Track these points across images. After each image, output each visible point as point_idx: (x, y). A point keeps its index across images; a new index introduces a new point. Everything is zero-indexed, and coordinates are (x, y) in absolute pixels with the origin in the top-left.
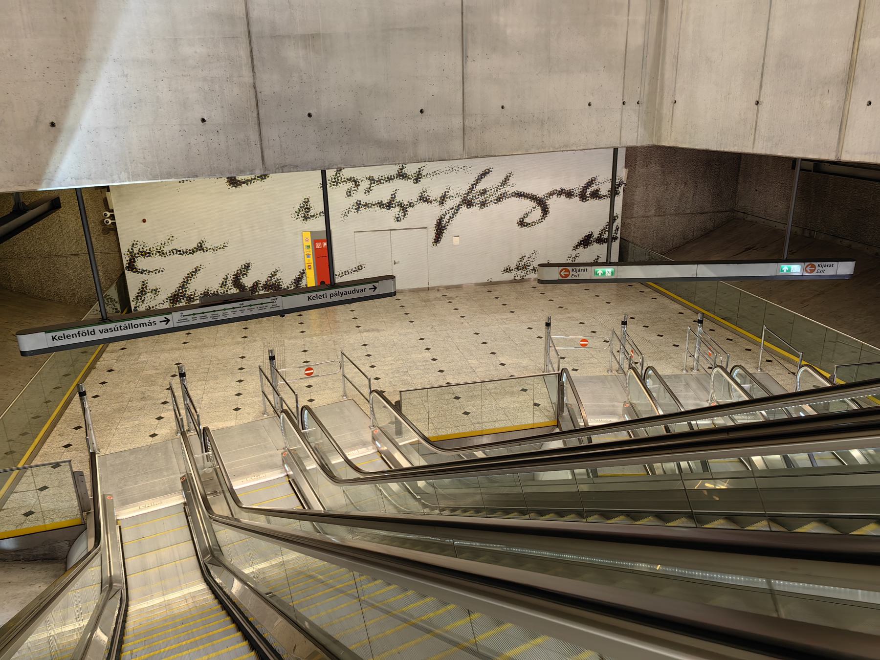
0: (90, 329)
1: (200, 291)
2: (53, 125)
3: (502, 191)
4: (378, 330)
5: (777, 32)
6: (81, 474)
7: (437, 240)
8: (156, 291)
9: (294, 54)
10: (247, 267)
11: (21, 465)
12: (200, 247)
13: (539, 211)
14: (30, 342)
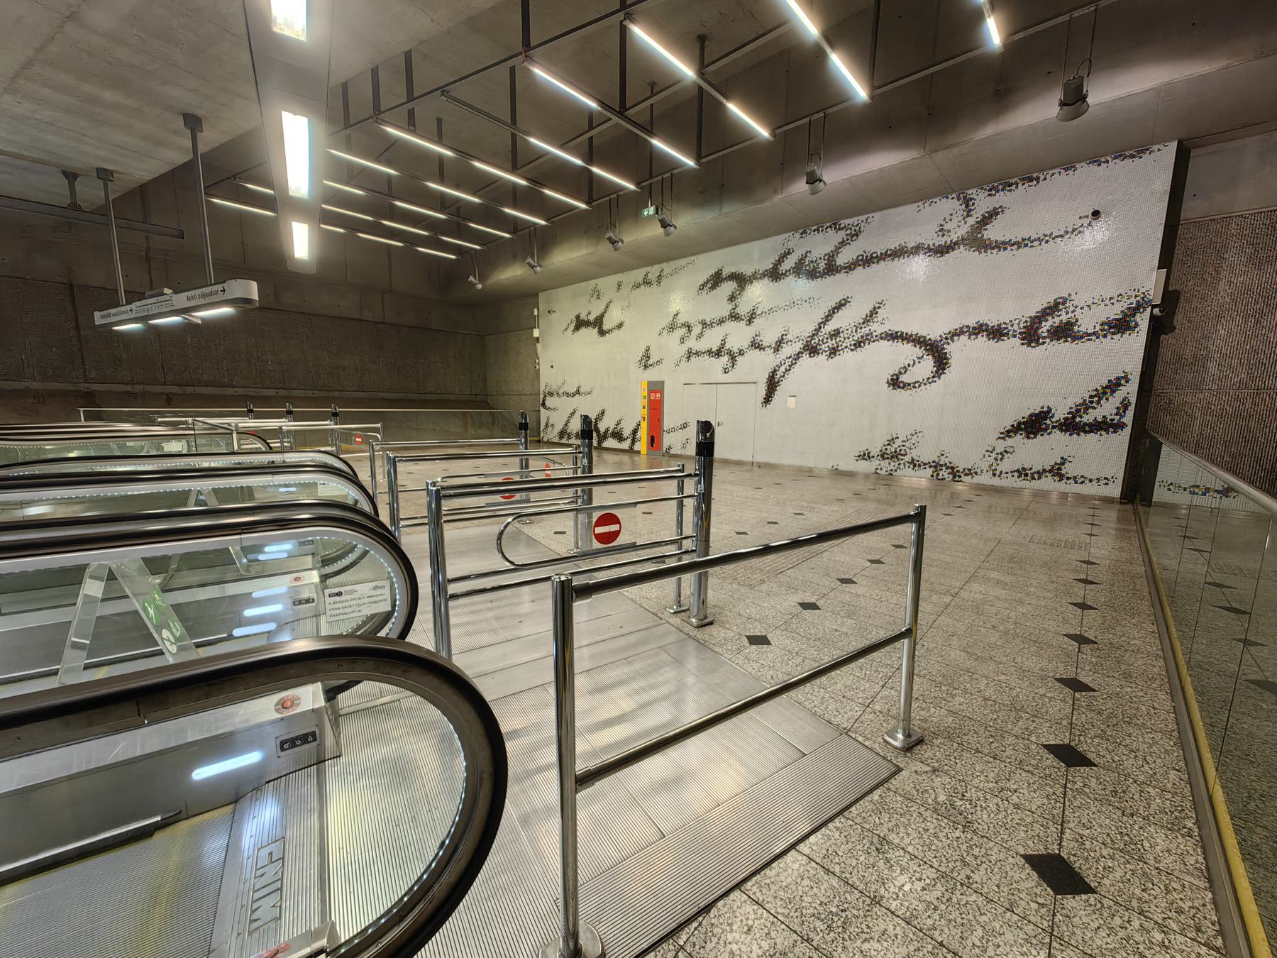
3: (865, 331)
7: (768, 399)
12: (578, 392)
13: (928, 364)
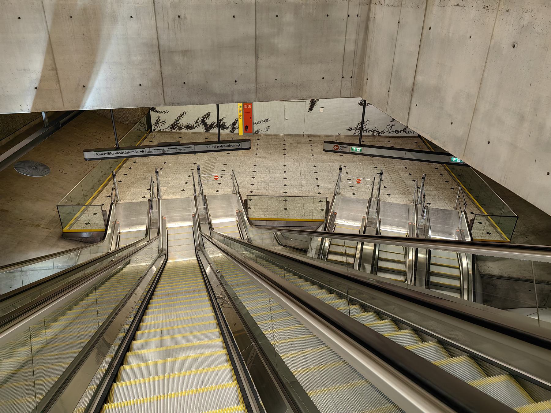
0: (112, 152)
1: (185, 124)
2: (84, 86)
4: (265, 158)
5: (396, 61)
6: (106, 211)
7: (311, 108)
8: (164, 122)
9: (178, 59)
10: (209, 114)
11: (86, 204)
14: (88, 155)
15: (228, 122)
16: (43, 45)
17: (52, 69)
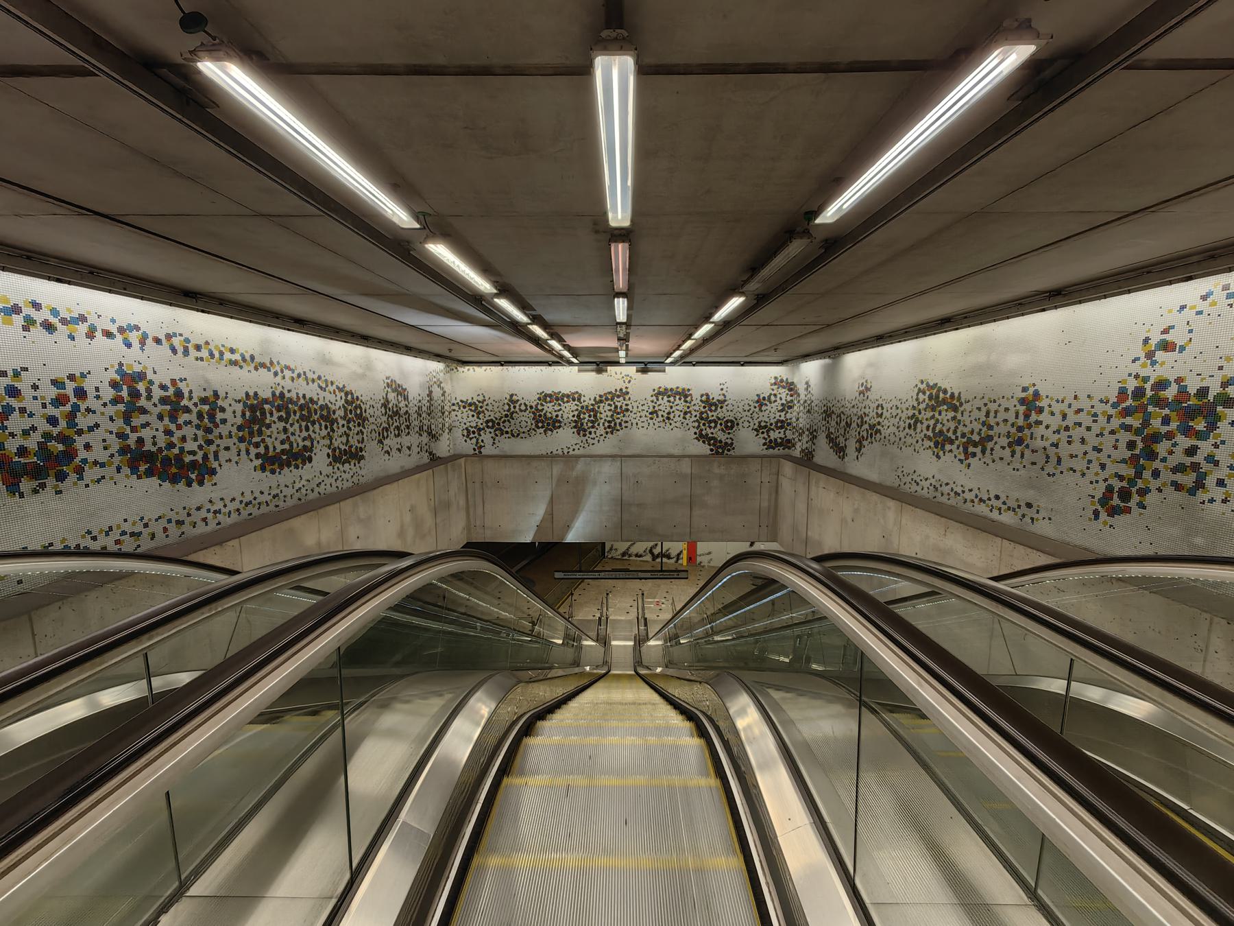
14: (557, 575)
15: (674, 553)
16: (547, 499)
17: (550, 515)
